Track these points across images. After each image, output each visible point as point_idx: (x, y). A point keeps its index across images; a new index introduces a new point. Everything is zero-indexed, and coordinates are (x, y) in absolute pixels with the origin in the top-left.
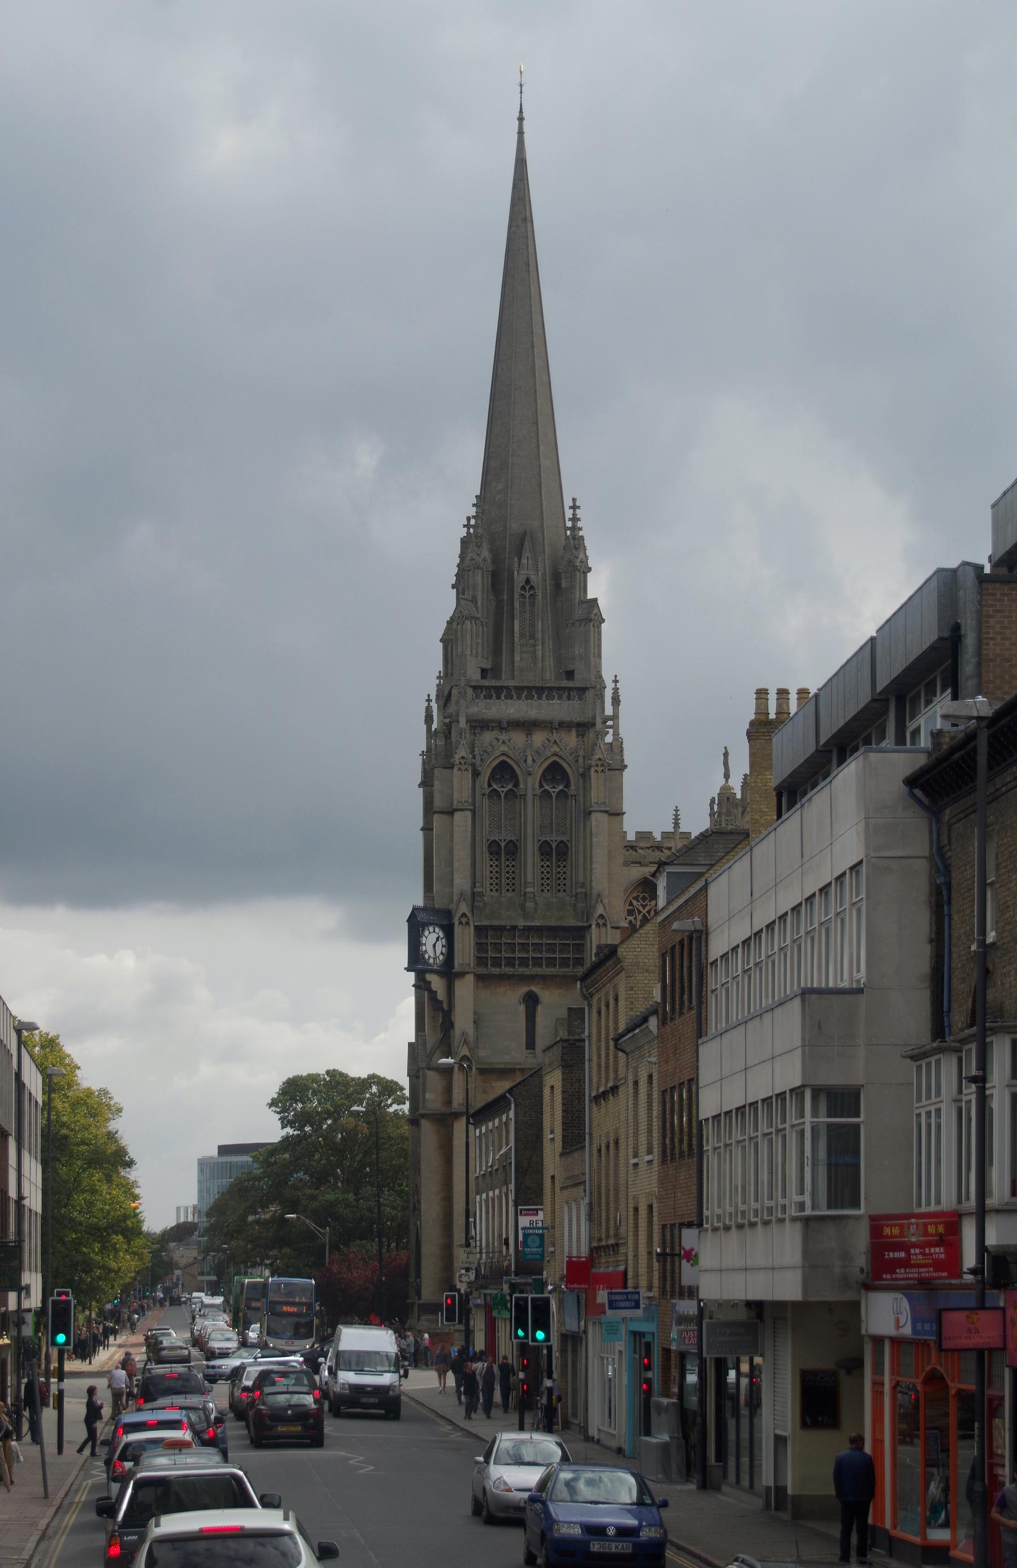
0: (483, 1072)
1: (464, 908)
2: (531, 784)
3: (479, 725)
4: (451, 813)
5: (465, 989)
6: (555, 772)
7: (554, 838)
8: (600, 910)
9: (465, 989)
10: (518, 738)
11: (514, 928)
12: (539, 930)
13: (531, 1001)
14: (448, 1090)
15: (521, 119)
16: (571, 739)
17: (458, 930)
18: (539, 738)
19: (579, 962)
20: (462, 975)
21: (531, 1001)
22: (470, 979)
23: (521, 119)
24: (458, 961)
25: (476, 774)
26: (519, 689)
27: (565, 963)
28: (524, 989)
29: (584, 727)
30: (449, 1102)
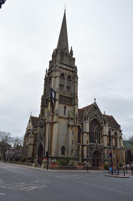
0: (59, 117)
1: (58, 90)
2: (66, 77)
3: (61, 67)
4: (56, 78)
5: (57, 102)
6: (69, 77)
7: (68, 86)
9: (57, 102)
10: (65, 71)
11: (63, 96)
12: (67, 97)
13: (65, 107)
14: (52, 119)
15: (65, 10)
16: (71, 73)
17: (57, 93)
18: (68, 72)
19: (72, 103)
20: (57, 100)
21: (65, 107)
22: (58, 101)
23: (65, 10)
24: (56, 99)
25: (60, 73)
26: (65, 65)
27: (70, 103)
28: (64, 105)
29: (73, 72)
30: (52, 121)
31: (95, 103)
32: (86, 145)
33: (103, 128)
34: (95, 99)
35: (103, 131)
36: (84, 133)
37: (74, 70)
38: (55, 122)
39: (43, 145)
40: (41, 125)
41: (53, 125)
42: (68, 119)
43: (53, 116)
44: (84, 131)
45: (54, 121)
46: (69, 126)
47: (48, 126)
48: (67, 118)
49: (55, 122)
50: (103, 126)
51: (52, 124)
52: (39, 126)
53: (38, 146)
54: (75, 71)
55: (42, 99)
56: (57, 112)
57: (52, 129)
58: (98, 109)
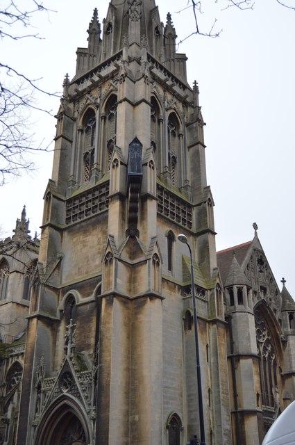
5: (152, 207)
8: (209, 197)
14: (132, 280)
31: (256, 239)
32: (253, 413)
33: (285, 342)
34: (255, 226)
35: (285, 353)
36: (239, 357)
37: (189, 98)
38: (152, 296)
39: (85, 410)
40: (46, 315)
41: (145, 302)
42: (186, 290)
43: (133, 268)
44: (242, 350)
45: (143, 289)
46: (189, 320)
47: (115, 316)
48: (180, 287)
49: (152, 296)
50: (287, 336)
51: (134, 304)
52: (39, 317)
53: (40, 415)
54: (193, 102)
55: (48, 197)
56: (156, 251)
57: (132, 330)
58: (267, 266)
